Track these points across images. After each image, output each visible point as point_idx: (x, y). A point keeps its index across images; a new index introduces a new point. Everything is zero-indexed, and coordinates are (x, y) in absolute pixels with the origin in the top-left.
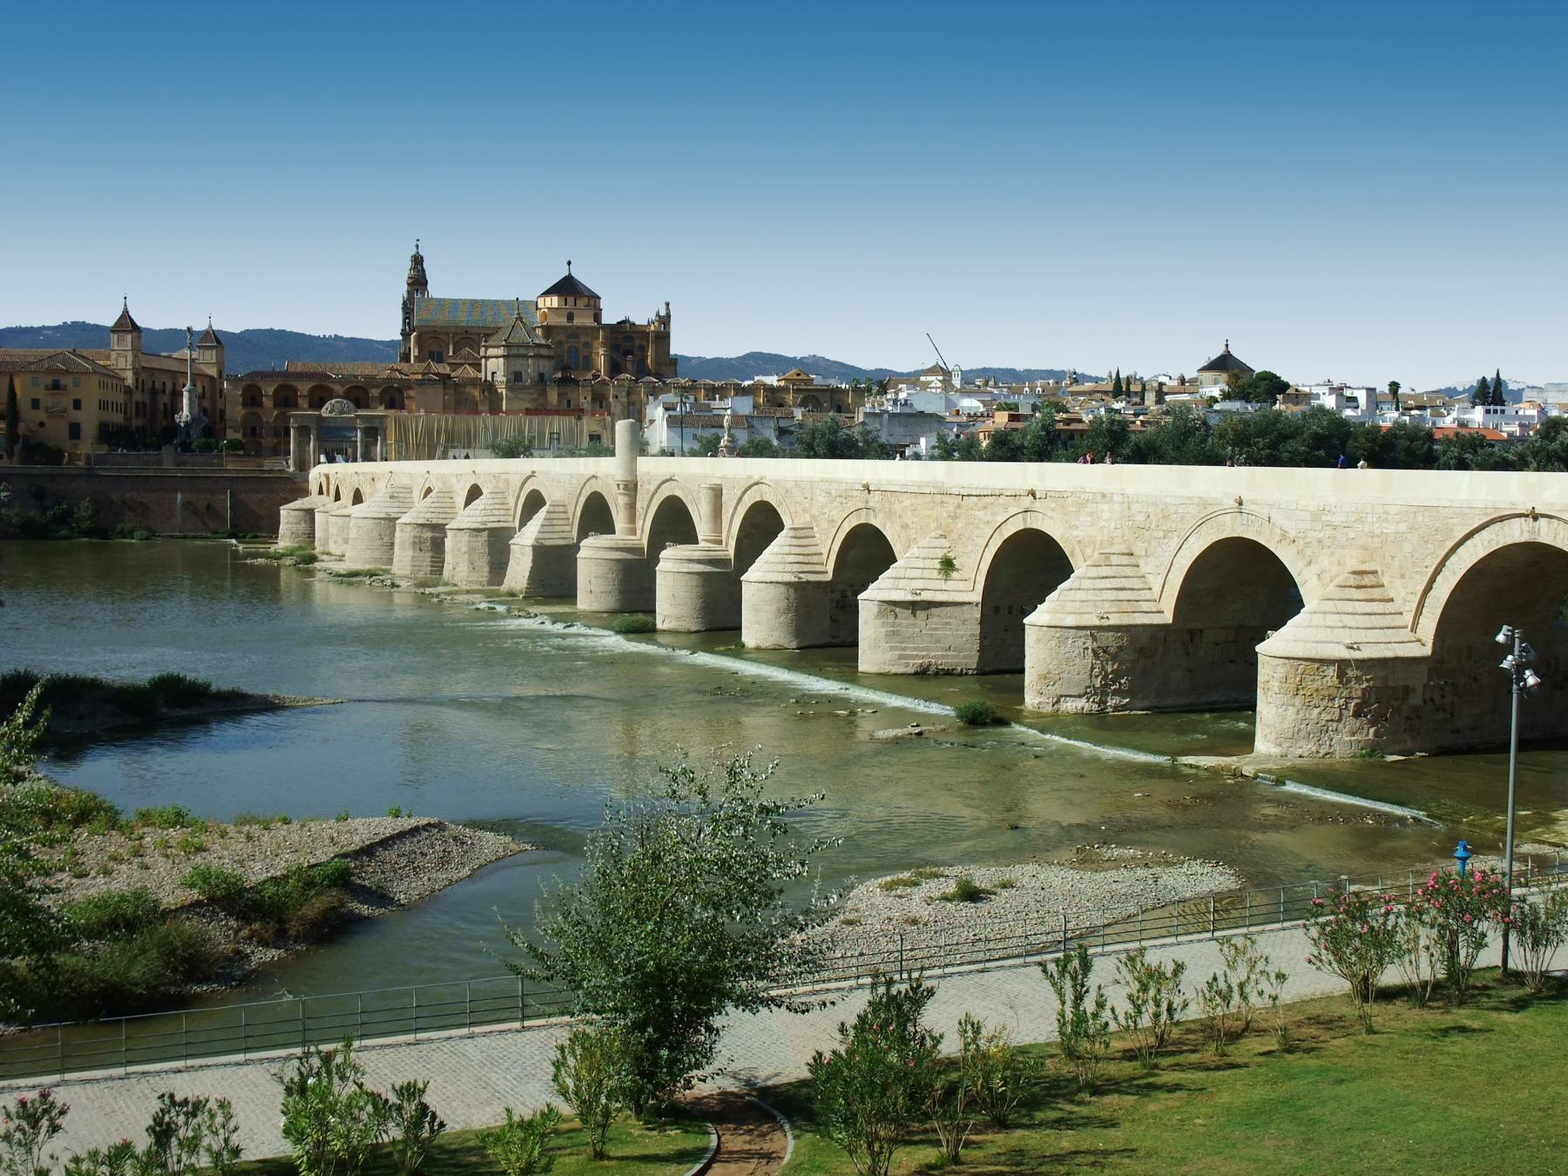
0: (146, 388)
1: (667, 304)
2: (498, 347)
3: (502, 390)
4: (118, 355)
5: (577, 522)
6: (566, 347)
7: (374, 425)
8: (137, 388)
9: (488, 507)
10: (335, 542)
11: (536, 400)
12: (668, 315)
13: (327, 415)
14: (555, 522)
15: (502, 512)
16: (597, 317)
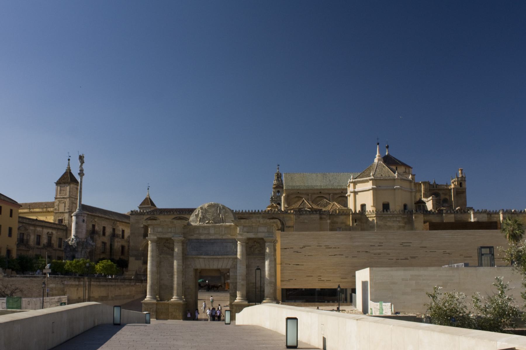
3: (372, 218)
7: (260, 235)
13: (197, 224)
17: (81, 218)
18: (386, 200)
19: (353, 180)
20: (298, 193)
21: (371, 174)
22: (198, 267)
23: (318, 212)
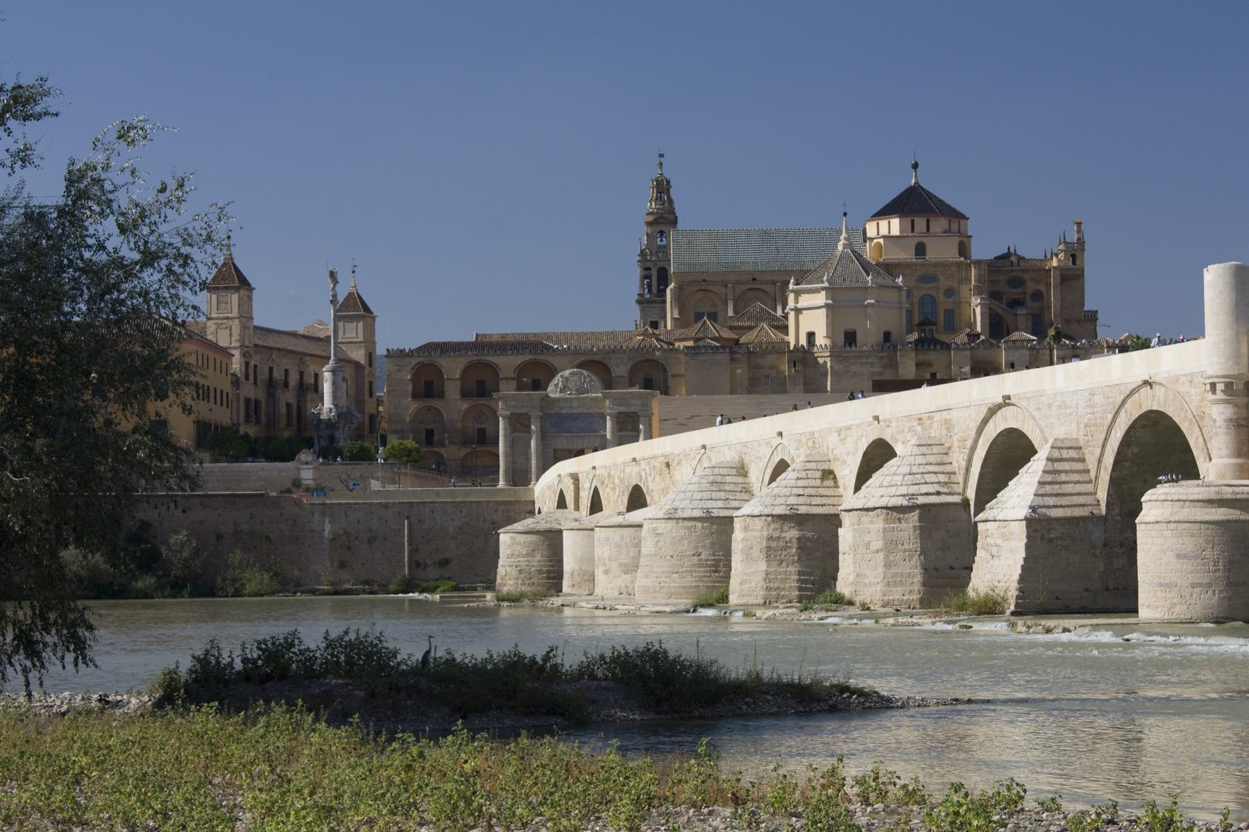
0: (260, 378)
1: (1079, 224)
3: (824, 359)
4: (218, 326)
5: (1105, 477)
7: (633, 409)
8: (247, 378)
9: (915, 469)
10: (607, 572)
12: (1081, 242)
13: (557, 395)
14: (1063, 477)
15: (942, 478)
17: (340, 375)
19: (795, 287)
20: (704, 280)
21: (825, 278)
23: (727, 350)
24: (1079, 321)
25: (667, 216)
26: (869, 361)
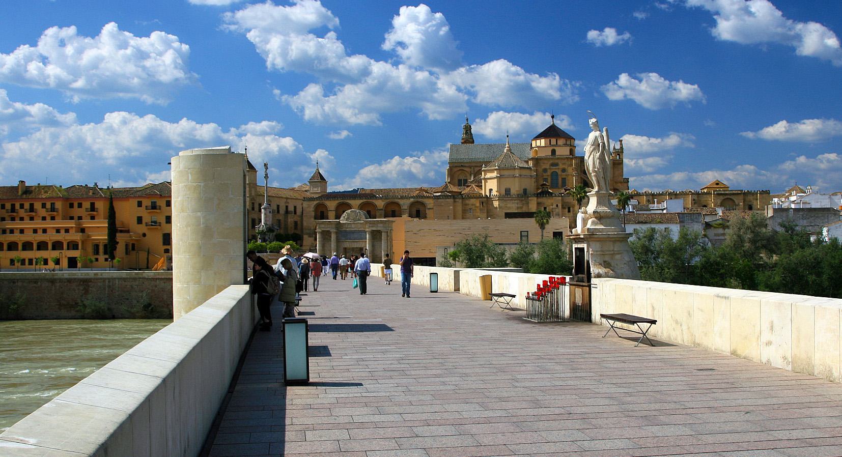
2: (492, 171)
6: (549, 173)
8: (253, 209)
11: (522, 208)
12: (622, 148)
13: (345, 222)
16: (572, 152)
18: (508, 186)
22: (346, 247)
24: (621, 182)
25: (469, 140)
26: (516, 202)
